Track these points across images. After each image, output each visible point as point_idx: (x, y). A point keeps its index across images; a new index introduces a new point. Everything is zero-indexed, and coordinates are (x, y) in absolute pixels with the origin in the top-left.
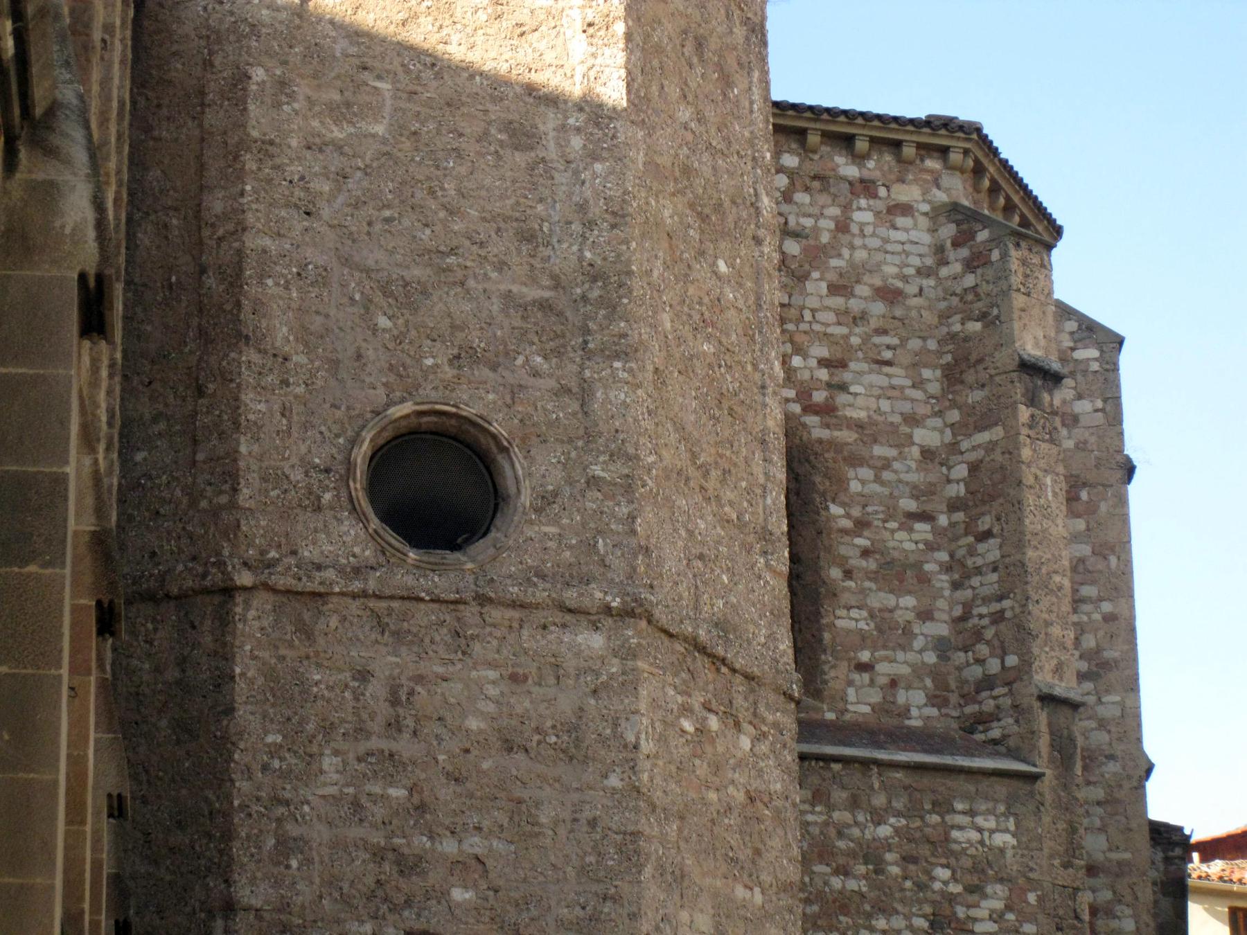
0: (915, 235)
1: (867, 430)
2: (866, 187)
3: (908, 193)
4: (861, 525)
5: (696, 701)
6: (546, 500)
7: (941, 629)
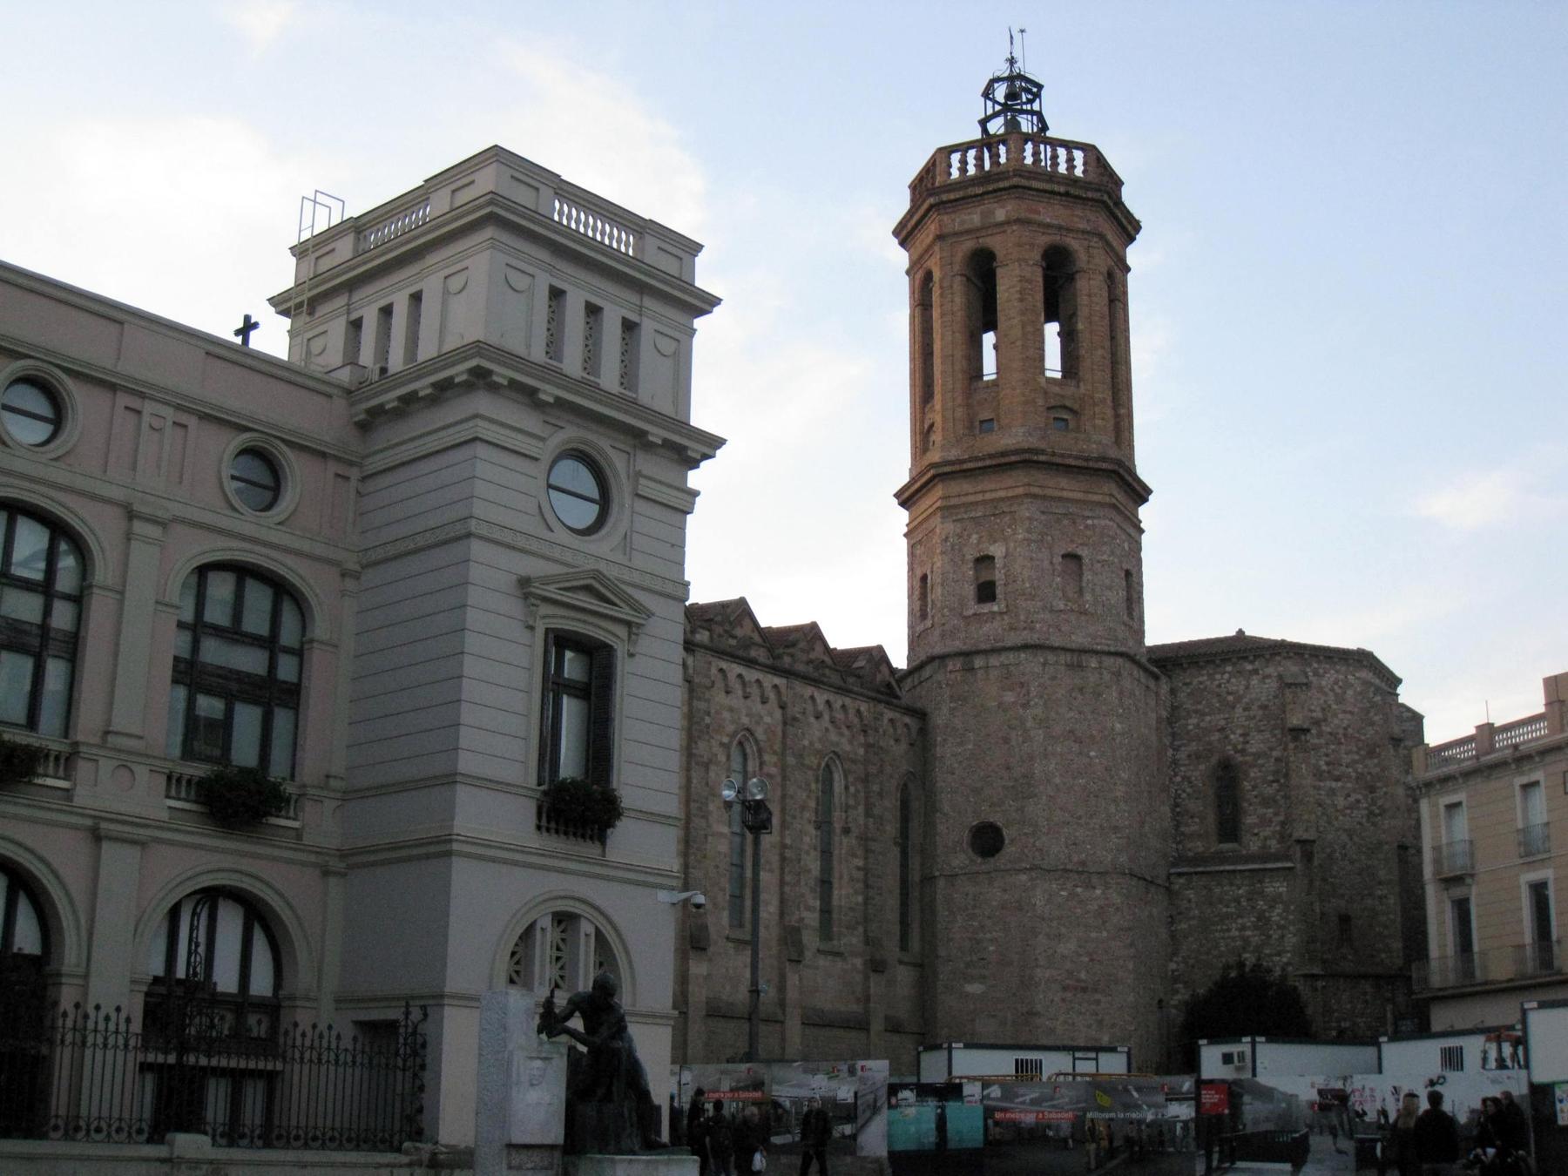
0: (1272, 684)
1: (1257, 755)
2: (1256, 672)
3: (1270, 670)
4: (1254, 787)
5: (1069, 885)
6: (1012, 841)
7: (1282, 818)
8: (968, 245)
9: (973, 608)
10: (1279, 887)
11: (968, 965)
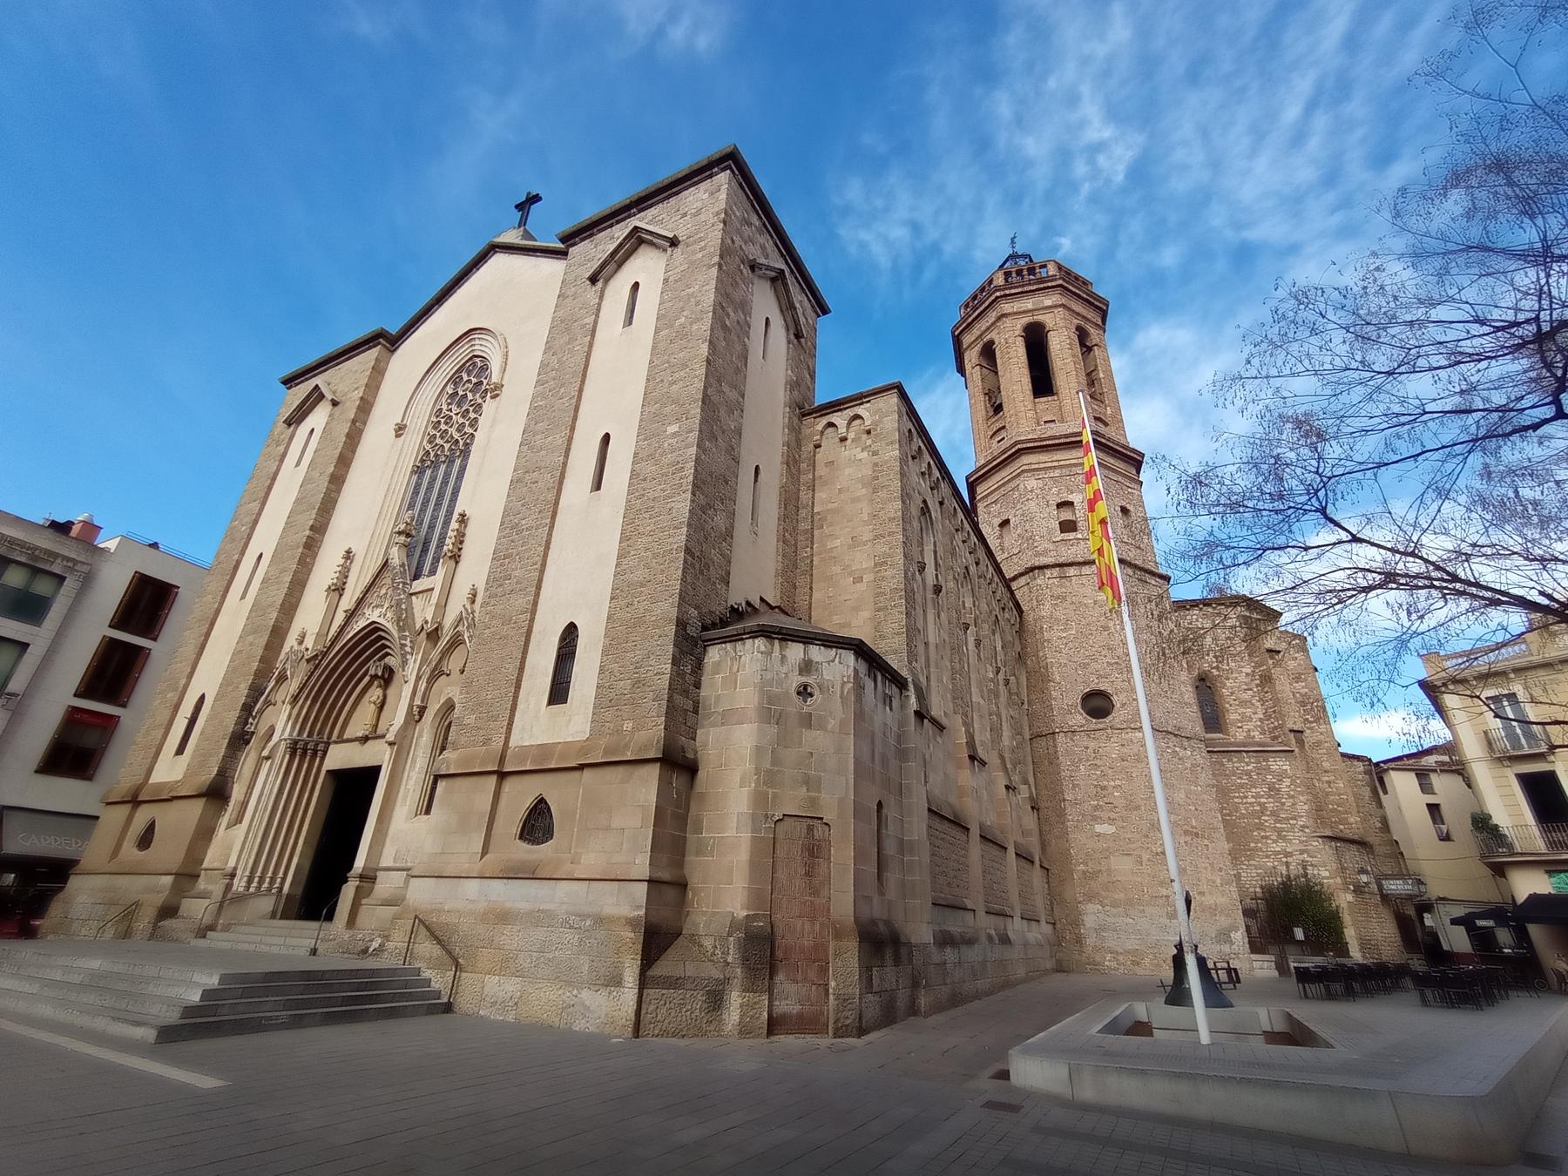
8: (1026, 320)
10: (1278, 764)
11: (1096, 808)
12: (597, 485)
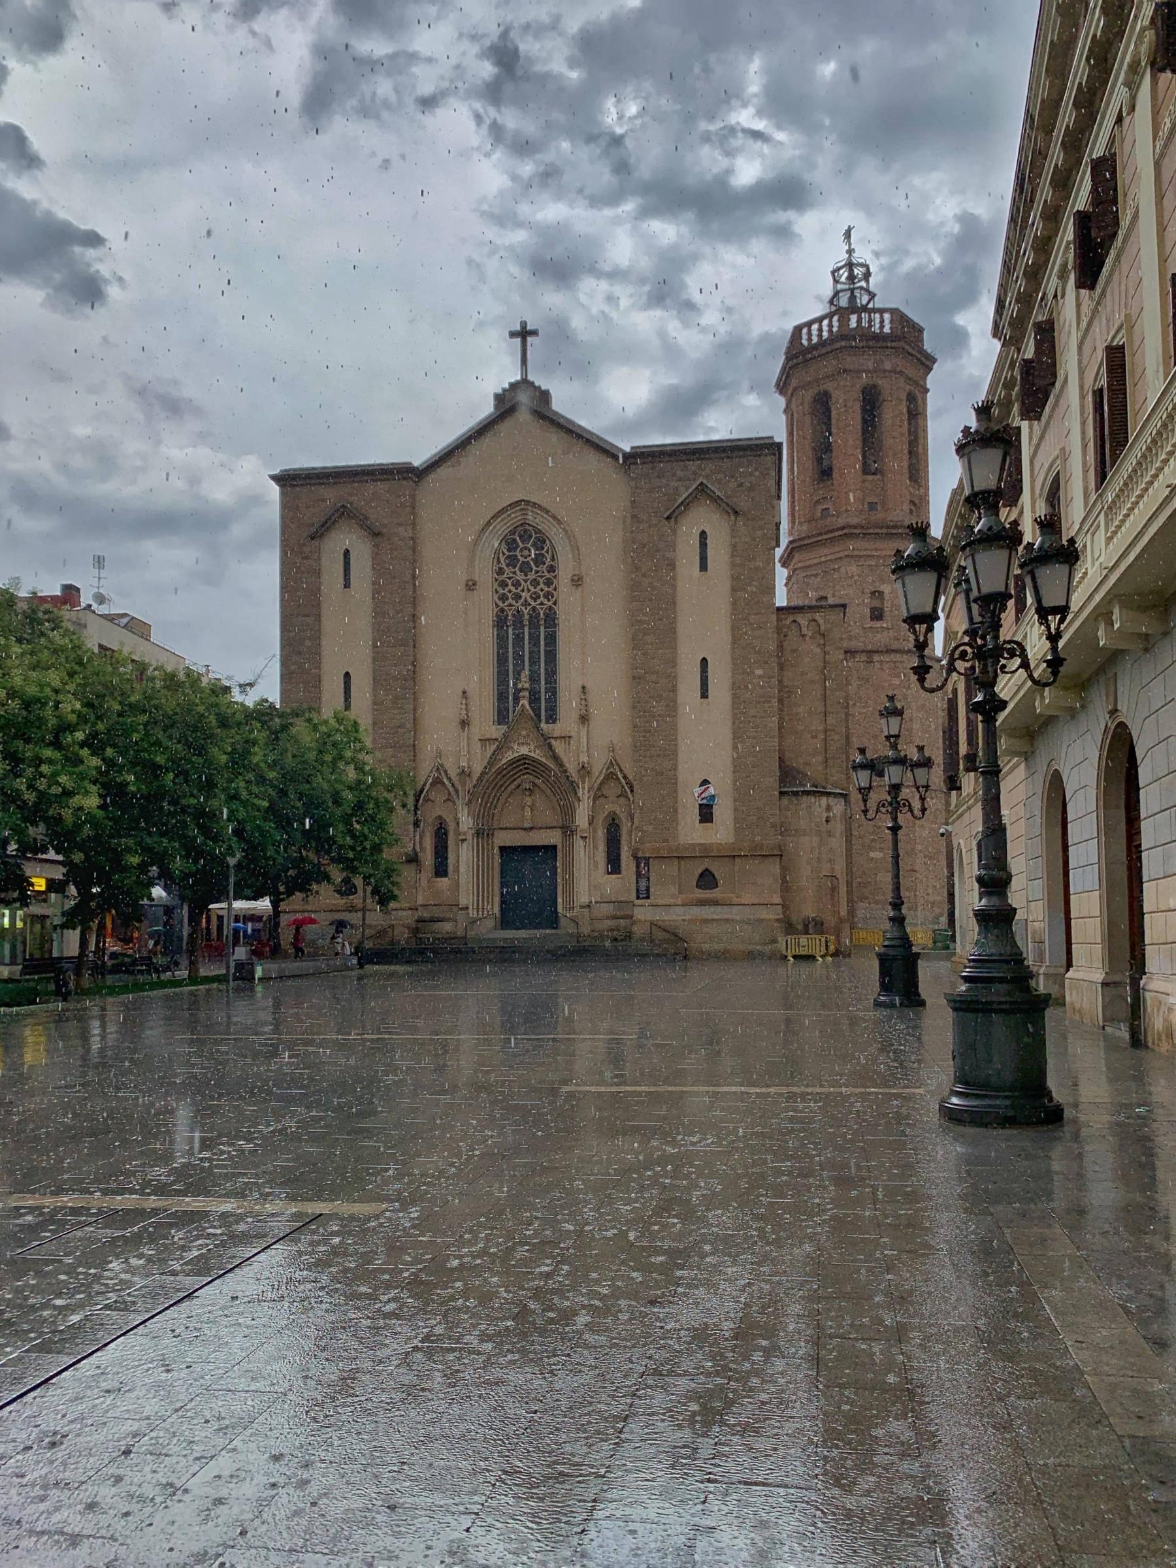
9: (869, 624)
11: (873, 840)
12: (704, 695)
